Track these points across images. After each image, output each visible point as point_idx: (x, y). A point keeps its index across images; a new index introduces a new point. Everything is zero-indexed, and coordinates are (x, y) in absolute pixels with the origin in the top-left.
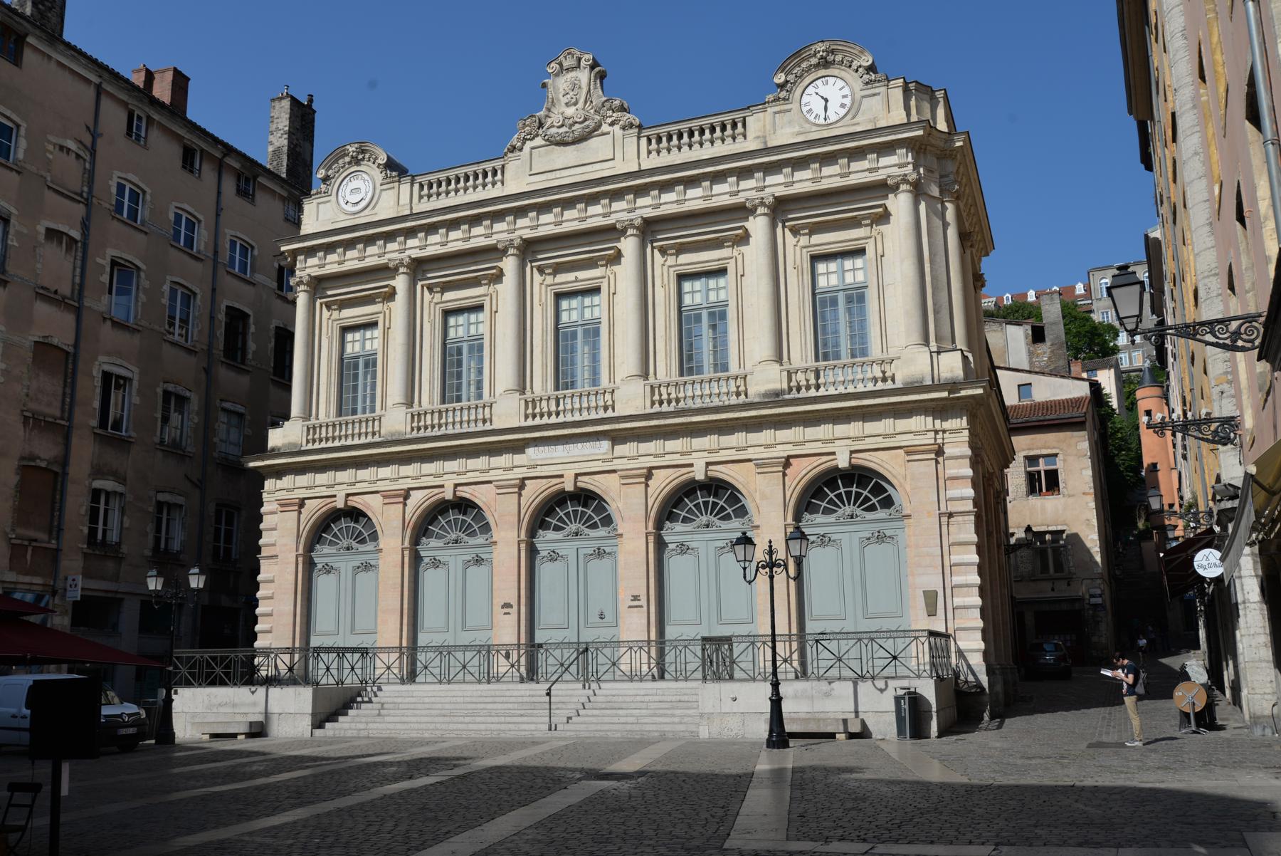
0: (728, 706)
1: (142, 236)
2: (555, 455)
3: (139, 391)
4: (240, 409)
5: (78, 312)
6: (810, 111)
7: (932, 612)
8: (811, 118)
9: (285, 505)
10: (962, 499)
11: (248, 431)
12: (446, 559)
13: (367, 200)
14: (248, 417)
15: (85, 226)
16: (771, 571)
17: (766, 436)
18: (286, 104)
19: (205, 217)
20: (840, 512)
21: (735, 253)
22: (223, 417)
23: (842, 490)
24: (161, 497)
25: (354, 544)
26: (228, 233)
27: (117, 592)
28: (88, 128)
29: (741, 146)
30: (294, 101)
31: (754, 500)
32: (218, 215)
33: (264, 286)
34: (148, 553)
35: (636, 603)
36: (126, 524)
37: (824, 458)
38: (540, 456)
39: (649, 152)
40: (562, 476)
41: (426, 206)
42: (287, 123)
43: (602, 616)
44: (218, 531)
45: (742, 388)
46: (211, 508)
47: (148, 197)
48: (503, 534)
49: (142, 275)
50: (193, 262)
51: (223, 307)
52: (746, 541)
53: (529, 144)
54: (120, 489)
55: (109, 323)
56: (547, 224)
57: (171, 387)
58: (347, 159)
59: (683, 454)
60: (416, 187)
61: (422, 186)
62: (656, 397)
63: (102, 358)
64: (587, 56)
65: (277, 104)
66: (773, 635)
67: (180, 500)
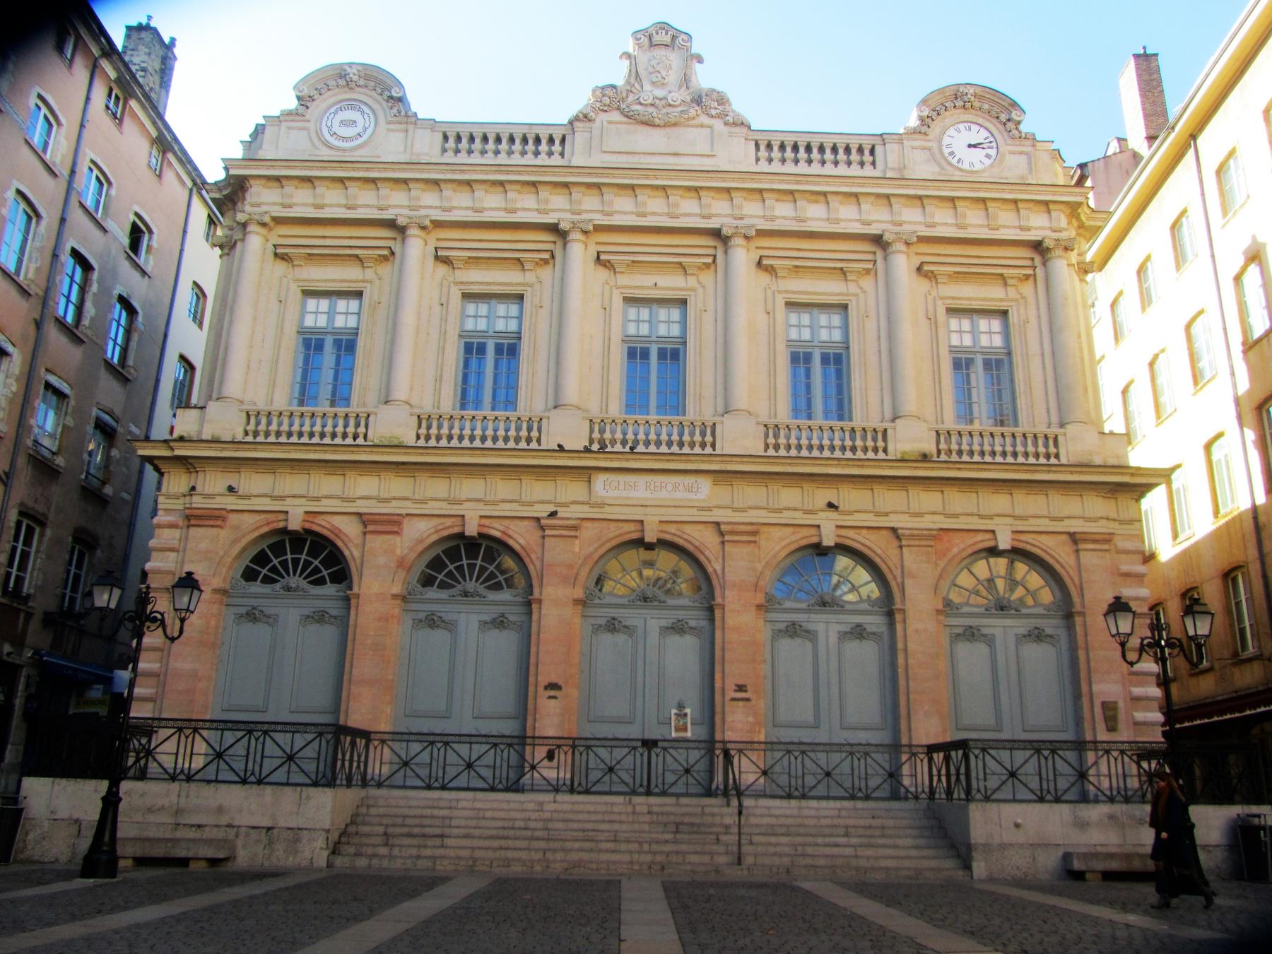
0: (1010, 836)
4: (65, 388)
6: (952, 153)
7: (1111, 728)
8: (954, 161)
9: (194, 519)
11: (70, 421)
13: (365, 137)
14: (73, 402)
26: (88, 154)
31: (895, 578)
32: (82, 126)
33: (115, 238)
35: (739, 695)
37: (980, 537)
38: (612, 493)
41: (449, 158)
44: (14, 549)
45: (880, 444)
51: (68, 249)
61: (446, 138)
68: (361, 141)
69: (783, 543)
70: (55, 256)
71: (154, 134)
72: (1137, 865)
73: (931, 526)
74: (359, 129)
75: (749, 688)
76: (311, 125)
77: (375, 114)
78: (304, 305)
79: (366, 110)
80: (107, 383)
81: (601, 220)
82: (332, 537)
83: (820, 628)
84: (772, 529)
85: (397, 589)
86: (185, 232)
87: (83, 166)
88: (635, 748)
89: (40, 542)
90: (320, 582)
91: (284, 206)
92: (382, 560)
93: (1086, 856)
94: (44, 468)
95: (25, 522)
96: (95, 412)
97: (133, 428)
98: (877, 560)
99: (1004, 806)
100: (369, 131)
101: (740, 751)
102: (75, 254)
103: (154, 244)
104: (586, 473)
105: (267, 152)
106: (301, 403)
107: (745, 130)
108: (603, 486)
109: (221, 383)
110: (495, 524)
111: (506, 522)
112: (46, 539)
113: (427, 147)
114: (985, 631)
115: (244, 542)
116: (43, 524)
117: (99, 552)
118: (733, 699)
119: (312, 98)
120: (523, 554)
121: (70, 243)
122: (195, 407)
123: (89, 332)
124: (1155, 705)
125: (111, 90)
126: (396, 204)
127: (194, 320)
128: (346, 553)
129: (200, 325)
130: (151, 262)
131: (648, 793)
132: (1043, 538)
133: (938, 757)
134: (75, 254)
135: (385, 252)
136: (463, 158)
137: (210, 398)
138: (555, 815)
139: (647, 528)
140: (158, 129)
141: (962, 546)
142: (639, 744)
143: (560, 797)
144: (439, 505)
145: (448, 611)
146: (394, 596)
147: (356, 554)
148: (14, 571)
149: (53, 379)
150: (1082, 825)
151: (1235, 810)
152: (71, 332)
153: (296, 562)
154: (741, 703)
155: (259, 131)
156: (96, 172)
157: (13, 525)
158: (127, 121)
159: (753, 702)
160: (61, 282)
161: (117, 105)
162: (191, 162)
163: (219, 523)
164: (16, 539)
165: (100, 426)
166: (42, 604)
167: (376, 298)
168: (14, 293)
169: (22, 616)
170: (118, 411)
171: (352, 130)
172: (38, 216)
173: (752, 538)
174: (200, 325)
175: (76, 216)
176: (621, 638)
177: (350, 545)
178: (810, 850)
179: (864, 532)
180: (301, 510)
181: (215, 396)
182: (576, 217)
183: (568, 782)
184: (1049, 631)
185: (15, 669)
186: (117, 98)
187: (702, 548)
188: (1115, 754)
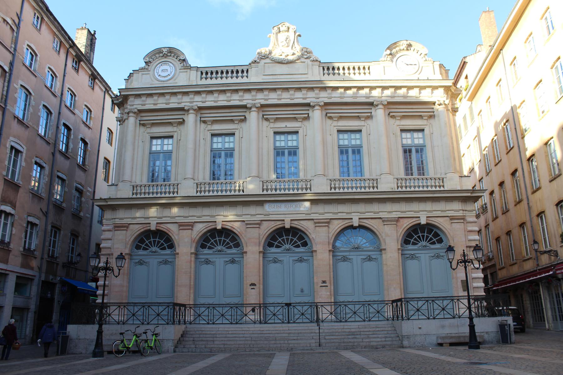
0: (418, 332)
1: (33, 77)
2: (280, 210)
3: (25, 160)
5: (4, 110)
10: (475, 240)
11: (66, 189)
12: (214, 260)
14: (67, 182)
15: (11, 64)
16: (465, 264)
17: (389, 207)
18: (85, 32)
19: (60, 75)
20: (420, 244)
21: (366, 124)
22: (57, 179)
23: (420, 234)
24: (31, 219)
25: (158, 250)
26: (67, 85)
27: (6, 270)
28: (17, 14)
29: (367, 77)
30: (89, 30)
31: (382, 237)
32: (64, 76)
33: (79, 116)
34: (22, 249)
36: (14, 232)
37: (414, 220)
38: (272, 210)
39: (324, 74)
40: (284, 220)
41: (204, 82)
42: (85, 41)
43: (302, 291)
44: (51, 240)
45: (375, 185)
46: (49, 228)
47: (38, 58)
49: (32, 98)
50: (52, 97)
51: (62, 123)
52: (450, 249)
53: (263, 61)
54: (13, 212)
55: (16, 119)
56: (273, 98)
57: (38, 160)
58: (161, 55)
59: (347, 213)
60: (200, 73)
61: (202, 73)
62: (333, 186)
63: (12, 138)
64: (293, 27)
65: (80, 31)
66: (469, 296)
67: (36, 221)
68: (169, 77)
69: (339, 226)
70: (58, 127)
71: (90, 73)
72: (462, 340)
74: (169, 73)
75: (327, 282)
76: (151, 73)
77: (174, 66)
78: (151, 142)
79: (171, 65)
80: (79, 173)
81: (263, 102)
82: (167, 232)
84: (334, 221)
85: (193, 251)
86: (103, 109)
87: (66, 90)
88: (283, 306)
89: (59, 236)
90: (164, 249)
91: (142, 105)
92: (186, 240)
93: (443, 338)
94: (58, 208)
95: (54, 229)
96: (75, 184)
97: (89, 189)
98: (375, 230)
99: (415, 322)
100: (173, 73)
101: (322, 306)
102: (65, 125)
103: (93, 116)
104: (261, 203)
105: (135, 84)
106: (152, 181)
107: (318, 63)
108: (268, 208)
109: (123, 175)
111: (232, 223)
112: (61, 235)
113: (194, 79)
114: (417, 255)
115: (135, 235)
116: (60, 230)
117: (80, 238)
118: (321, 286)
119: (150, 62)
120: (239, 235)
121: (62, 121)
122: (113, 185)
123: (71, 154)
124: (482, 280)
125: (74, 59)
126: (185, 102)
127: (109, 143)
129: (111, 145)
130: (92, 123)
131: (289, 323)
132: (439, 219)
133: (395, 304)
134: (65, 125)
135: (181, 120)
136: (209, 82)
137: (119, 181)
138: (254, 332)
139: (286, 222)
140: (91, 71)
141: (408, 223)
143: (256, 325)
144: (205, 219)
145: (211, 258)
146: (192, 253)
147: (177, 238)
148: (51, 248)
149: (60, 174)
150: (443, 327)
151: (500, 318)
152: (65, 155)
153: (154, 241)
155: (131, 75)
156: (70, 92)
157: (50, 231)
158: (80, 70)
159: (329, 287)
160: (60, 136)
161: (76, 64)
162: (104, 81)
163: (125, 229)
164: (51, 237)
165: (77, 189)
166: (62, 260)
167: (179, 138)
168: (44, 143)
169: (55, 265)
170: (83, 183)
171: (165, 72)
172: (51, 113)
174: (111, 145)
175: (64, 111)
177: (174, 235)
178: (345, 340)
179: (370, 220)
180: (155, 222)
181: (121, 180)
182: (254, 102)
184: (441, 254)
185: (54, 285)
186: (76, 62)
188: (456, 301)
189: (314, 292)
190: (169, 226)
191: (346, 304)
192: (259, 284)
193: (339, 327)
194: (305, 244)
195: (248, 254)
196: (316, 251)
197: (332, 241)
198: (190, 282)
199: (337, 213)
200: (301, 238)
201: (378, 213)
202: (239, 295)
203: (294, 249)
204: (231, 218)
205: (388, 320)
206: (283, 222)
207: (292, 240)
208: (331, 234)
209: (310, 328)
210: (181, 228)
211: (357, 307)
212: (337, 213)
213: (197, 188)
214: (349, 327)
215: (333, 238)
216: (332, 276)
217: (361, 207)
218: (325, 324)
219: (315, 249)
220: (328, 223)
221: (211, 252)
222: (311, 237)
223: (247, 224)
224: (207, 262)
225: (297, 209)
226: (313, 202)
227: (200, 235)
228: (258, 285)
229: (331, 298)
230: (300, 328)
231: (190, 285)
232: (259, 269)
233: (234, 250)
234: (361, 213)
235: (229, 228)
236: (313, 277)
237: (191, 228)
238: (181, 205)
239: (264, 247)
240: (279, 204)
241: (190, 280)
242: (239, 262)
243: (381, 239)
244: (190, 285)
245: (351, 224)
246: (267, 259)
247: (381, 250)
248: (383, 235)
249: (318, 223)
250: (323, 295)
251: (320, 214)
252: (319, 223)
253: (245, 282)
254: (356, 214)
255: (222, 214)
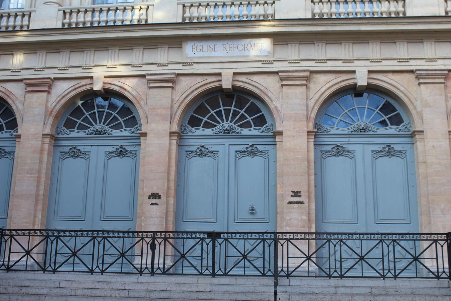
2: (213, 54)
17: (429, 50)
31: (415, 108)
40: (220, 74)
43: (252, 211)
48: (153, 126)
69: (328, 86)
73: (443, 68)
75: (302, 194)
82: (5, 97)
83: (358, 149)
85: (48, 131)
104: (176, 42)
108: (191, 51)
110: (116, 81)
111: (123, 80)
118: (290, 203)
128: (14, 107)
131: (213, 275)
139: (224, 78)
142: (205, 236)
145: (83, 146)
146: (44, 136)
147: (20, 107)
154: (296, 206)
159: (306, 204)
173: (304, 82)
176: (207, 160)
177: (17, 102)
179: (390, 75)
183: (149, 266)
187: (265, 90)
189: (276, 213)
190: (9, 86)
191: (342, 238)
192: (168, 195)
193: (325, 290)
194: (261, 121)
195: (149, 137)
196: (281, 133)
197: (313, 115)
198: (38, 190)
199: (324, 61)
200: (253, 110)
201: (407, 60)
202: (129, 218)
203: (239, 129)
204: (120, 70)
205: (438, 277)
206: (218, 78)
207: (235, 114)
208: (313, 101)
209: (260, 289)
210: (29, 89)
211: (367, 245)
212: (324, 61)
213: (65, 18)
214: (348, 291)
215: (317, 108)
216: (313, 183)
217: (373, 50)
218: (294, 282)
219: (279, 129)
220: (307, 79)
221: (83, 135)
222: (272, 107)
223: (153, 82)
224: (75, 153)
225: (246, 53)
226: (279, 39)
227: (63, 101)
228: (164, 198)
229: (310, 227)
230: (237, 289)
231: (37, 196)
232: (169, 166)
233: (125, 132)
234: (372, 61)
235: (117, 89)
236: (275, 185)
237: (46, 88)
238: (29, 48)
239: (181, 125)
240: (211, 44)
241: (38, 186)
242: (134, 155)
243: (413, 112)
244: (37, 196)
245: (352, 82)
246: (187, 148)
247: (413, 135)
248: (418, 104)
249: (286, 79)
250: (294, 219)
251: (291, 62)
252: (288, 78)
253: (140, 191)
254: (362, 64)
255: (105, 63)
